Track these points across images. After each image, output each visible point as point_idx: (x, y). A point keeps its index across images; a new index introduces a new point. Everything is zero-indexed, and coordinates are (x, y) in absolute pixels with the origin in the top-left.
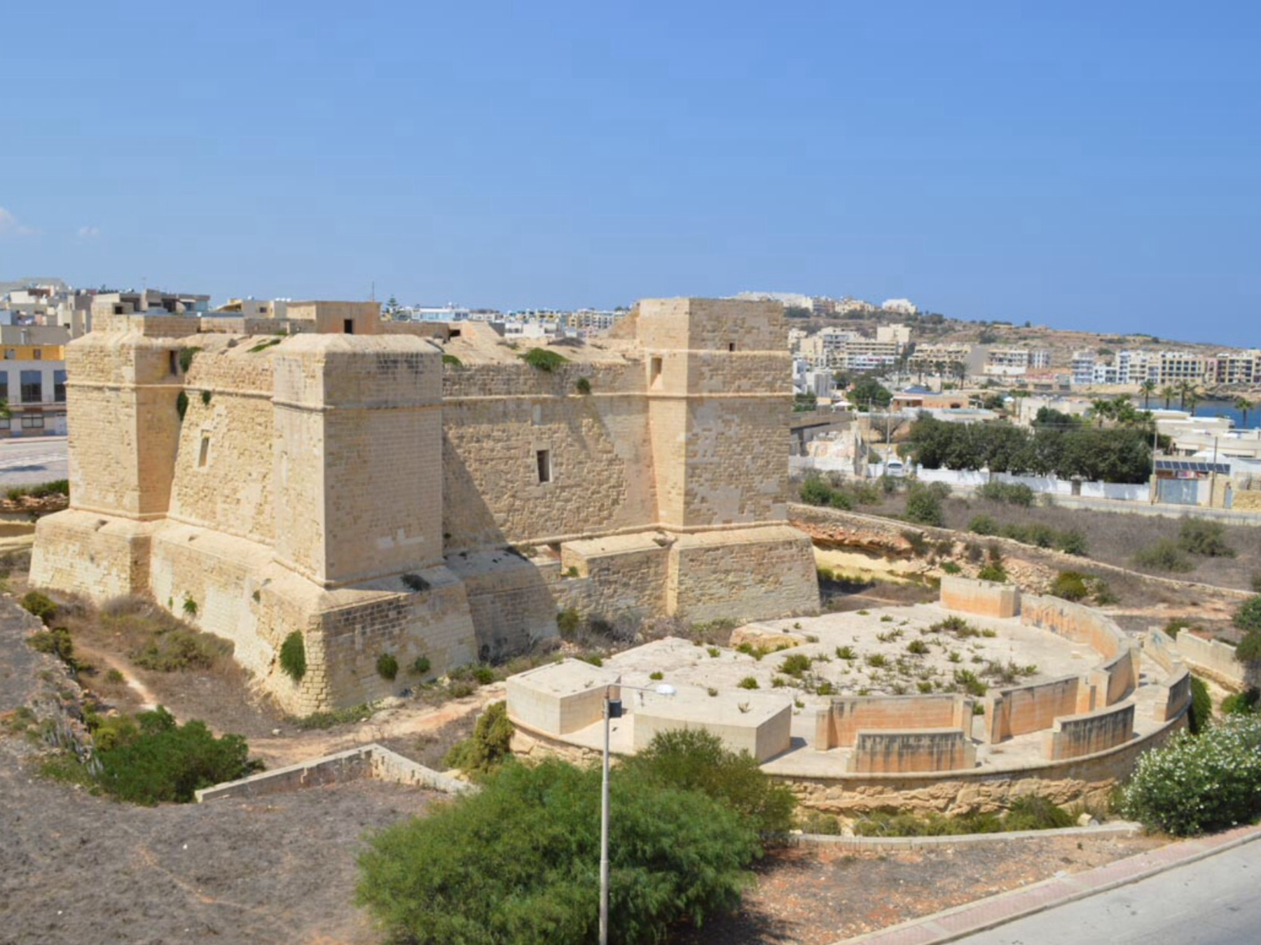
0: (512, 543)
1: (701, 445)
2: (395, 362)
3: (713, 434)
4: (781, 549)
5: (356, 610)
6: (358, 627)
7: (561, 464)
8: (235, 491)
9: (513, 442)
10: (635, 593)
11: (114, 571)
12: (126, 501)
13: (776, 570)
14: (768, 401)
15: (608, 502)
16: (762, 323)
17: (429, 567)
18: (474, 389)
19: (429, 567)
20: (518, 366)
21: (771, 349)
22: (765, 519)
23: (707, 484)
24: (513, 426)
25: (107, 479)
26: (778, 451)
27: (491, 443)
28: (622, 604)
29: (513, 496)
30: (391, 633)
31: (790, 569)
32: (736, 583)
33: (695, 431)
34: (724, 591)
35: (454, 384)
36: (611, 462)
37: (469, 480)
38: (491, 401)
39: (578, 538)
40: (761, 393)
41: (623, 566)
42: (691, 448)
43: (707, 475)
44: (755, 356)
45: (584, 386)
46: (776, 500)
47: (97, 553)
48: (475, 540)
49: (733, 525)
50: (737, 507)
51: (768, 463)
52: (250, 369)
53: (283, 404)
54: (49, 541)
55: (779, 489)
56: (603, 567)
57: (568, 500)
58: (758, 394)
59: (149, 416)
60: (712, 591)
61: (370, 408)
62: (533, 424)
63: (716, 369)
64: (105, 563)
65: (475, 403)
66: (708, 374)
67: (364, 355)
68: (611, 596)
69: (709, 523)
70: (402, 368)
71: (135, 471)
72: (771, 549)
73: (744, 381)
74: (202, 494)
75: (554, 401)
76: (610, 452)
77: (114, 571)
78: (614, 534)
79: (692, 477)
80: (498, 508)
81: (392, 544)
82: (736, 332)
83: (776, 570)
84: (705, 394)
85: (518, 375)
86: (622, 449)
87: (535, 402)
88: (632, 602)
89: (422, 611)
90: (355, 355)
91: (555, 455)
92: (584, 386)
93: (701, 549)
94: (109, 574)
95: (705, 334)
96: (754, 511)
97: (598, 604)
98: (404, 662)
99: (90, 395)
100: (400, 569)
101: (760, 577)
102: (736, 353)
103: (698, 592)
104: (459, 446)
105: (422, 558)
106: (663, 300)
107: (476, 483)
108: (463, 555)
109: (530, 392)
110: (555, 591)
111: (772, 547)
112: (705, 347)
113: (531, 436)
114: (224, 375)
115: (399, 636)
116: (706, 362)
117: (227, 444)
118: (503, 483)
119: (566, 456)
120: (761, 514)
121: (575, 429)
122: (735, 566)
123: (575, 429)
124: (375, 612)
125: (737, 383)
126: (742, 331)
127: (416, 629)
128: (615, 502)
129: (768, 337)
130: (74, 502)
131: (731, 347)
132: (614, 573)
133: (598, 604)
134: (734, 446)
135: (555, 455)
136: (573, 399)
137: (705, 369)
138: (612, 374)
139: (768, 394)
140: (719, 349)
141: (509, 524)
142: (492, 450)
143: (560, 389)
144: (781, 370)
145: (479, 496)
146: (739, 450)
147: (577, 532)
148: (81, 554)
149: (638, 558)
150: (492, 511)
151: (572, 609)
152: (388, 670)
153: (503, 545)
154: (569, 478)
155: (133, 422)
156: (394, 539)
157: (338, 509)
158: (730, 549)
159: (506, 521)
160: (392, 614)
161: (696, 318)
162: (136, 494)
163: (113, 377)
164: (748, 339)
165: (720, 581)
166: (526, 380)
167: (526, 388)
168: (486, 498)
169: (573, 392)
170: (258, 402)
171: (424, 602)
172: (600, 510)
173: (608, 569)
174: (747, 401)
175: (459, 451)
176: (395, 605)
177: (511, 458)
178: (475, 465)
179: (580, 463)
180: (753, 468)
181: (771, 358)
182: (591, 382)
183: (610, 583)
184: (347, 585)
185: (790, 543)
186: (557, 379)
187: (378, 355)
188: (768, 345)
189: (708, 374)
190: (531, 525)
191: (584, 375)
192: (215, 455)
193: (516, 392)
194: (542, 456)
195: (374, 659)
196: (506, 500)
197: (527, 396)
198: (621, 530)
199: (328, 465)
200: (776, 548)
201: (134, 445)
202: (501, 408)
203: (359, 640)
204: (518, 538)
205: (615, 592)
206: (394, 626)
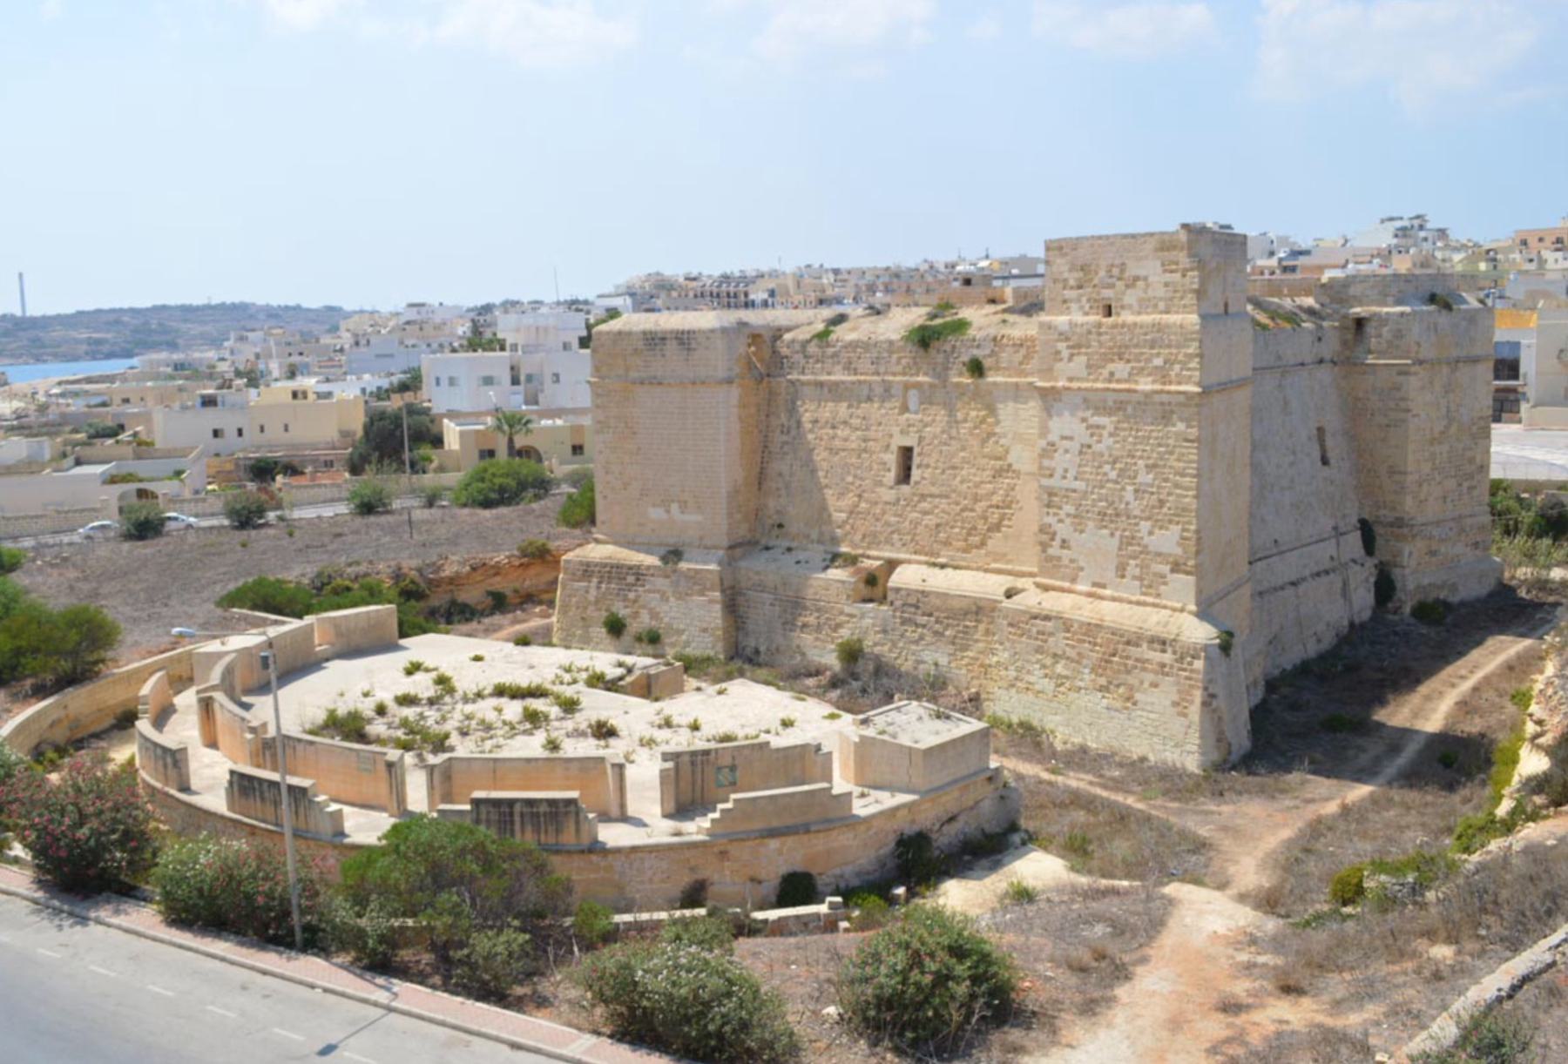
0: (844, 549)
1: (1060, 461)
2: (663, 339)
3: (1075, 446)
4: (1145, 645)
5: (596, 565)
6: (595, 580)
7: (928, 466)
9: (871, 434)
10: (951, 649)
13: (1131, 680)
14: (1157, 398)
15: (982, 527)
16: (1151, 269)
17: (706, 547)
18: (839, 367)
19: (706, 547)
20: (891, 343)
21: (1167, 312)
22: (1158, 595)
23: (1068, 521)
24: (874, 410)
26: (1177, 486)
27: (847, 432)
28: (928, 656)
29: (860, 496)
31: (1155, 685)
32: (1067, 677)
33: (1053, 437)
34: (1048, 685)
35: (817, 361)
36: (998, 473)
37: (814, 471)
38: (853, 383)
39: (927, 563)
40: (1145, 385)
41: (938, 609)
42: (1046, 463)
44: (1135, 324)
45: (977, 368)
46: (1176, 568)
48: (808, 536)
49: (1107, 592)
50: (1113, 567)
51: (1162, 503)
55: (1179, 551)
56: (918, 604)
57: (926, 513)
58: (1140, 387)
60: (1032, 679)
61: (634, 383)
62: (905, 409)
63: (1079, 346)
65: (837, 384)
66: (1065, 354)
67: (629, 334)
68: (916, 642)
69: (1074, 580)
70: (672, 346)
72: (1128, 643)
73: (1121, 369)
75: (931, 386)
76: (999, 459)
78: (978, 569)
79: (1048, 506)
80: (838, 507)
81: (664, 516)
82: (1112, 286)
83: (1131, 680)
84: (1060, 384)
85: (891, 352)
86: (1022, 458)
87: (907, 387)
88: (943, 661)
89: (661, 583)
90: (620, 333)
91: (920, 454)
92: (977, 368)
93: (1024, 612)
95: (1069, 294)
96: (1141, 579)
97: (894, 645)
98: (634, 627)
100: (671, 541)
101: (1103, 681)
102: (1111, 320)
103: (1013, 674)
104: (811, 431)
105: (701, 538)
107: (821, 474)
108: (789, 549)
109: (904, 374)
110: (842, 613)
111: (1133, 641)
112: (1068, 311)
113: (894, 427)
115: (635, 601)
116: (1064, 337)
118: (850, 479)
119: (935, 456)
120: (1151, 584)
121: (953, 422)
122: (1071, 653)
123: (953, 422)
124: (614, 572)
125: (1111, 367)
126: (1120, 285)
127: (653, 600)
128: (997, 527)
129: (1161, 292)
131: (1108, 311)
132: (924, 614)
133: (894, 645)
134: (1107, 468)
135: (920, 454)
136: (958, 385)
137: (1062, 346)
138: (1023, 351)
139: (1158, 387)
140: (1087, 314)
141: (848, 527)
142: (846, 440)
143: (942, 374)
144: (1179, 346)
145: (821, 489)
146: (1113, 475)
147: (932, 554)
149: (964, 604)
150: (832, 509)
151: (860, 641)
152: (615, 628)
153: (835, 550)
154: (933, 484)
156: (668, 512)
158: (1067, 625)
159: (845, 522)
160: (631, 579)
161: (1054, 269)
164: (1130, 298)
165: (1044, 667)
166: (898, 362)
167: (899, 368)
168: (828, 492)
169: (961, 374)
171: (667, 577)
172: (969, 534)
173: (917, 607)
174: (1123, 396)
175: (810, 437)
176: (638, 573)
177: (865, 450)
178: (825, 454)
179: (954, 468)
180: (1136, 507)
181: (1159, 328)
182: (987, 363)
183: (917, 625)
184: (615, 543)
185: (1164, 643)
186: (940, 358)
187: (644, 333)
188: (1162, 305)
189: (1065, 354)
190: (874, 535)
191: (976, 352)
193: (886, 373)
194: (907, 453)
195: (605, 614)
196: (850, 499)
197: (898, 378)
198: (994, 565)
200: (1137, 645)
202: (865, 392)
203: (593, 592)
204: (855, 546)
205: (921, 638)
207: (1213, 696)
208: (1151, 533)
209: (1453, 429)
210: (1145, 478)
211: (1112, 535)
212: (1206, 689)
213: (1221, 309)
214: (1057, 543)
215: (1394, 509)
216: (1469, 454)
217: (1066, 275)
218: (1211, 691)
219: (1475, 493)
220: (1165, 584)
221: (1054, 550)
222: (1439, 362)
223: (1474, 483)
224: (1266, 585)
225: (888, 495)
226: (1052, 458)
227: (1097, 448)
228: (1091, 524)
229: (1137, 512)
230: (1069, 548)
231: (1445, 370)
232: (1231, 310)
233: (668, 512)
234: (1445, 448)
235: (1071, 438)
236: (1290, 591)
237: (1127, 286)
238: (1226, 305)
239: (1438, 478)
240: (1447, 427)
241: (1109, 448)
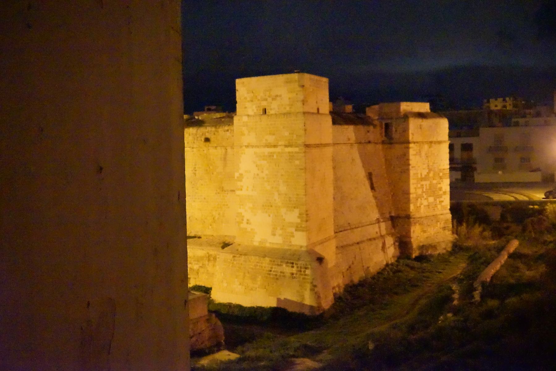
55: (299, 221)
66: (246, 132)
82: (266, 100)
189: (246, 132)
207: (315, 286)
209: (431, 175)
211: (269, 216)
212: (312, 283)
213: (316, 111)
214: (245, 221)
215: (405, 210)
216: (439, 186)
218: (314, 284)
219: (443, 204)
220: (293, 236)
221: (244, 225)
222: (423, 142)
223: (442, 199)
224: (345, 243)
226: (241, 181)
229: (280, 204)
230: (250, 224)
231: (426, 147)
232: (321, 111)
234: (428, 183)
236: (357, 246)
237: (273, 99)
238: (318, 109)
239: (425, 197)
240: (429, 173)
241: (267, 175)
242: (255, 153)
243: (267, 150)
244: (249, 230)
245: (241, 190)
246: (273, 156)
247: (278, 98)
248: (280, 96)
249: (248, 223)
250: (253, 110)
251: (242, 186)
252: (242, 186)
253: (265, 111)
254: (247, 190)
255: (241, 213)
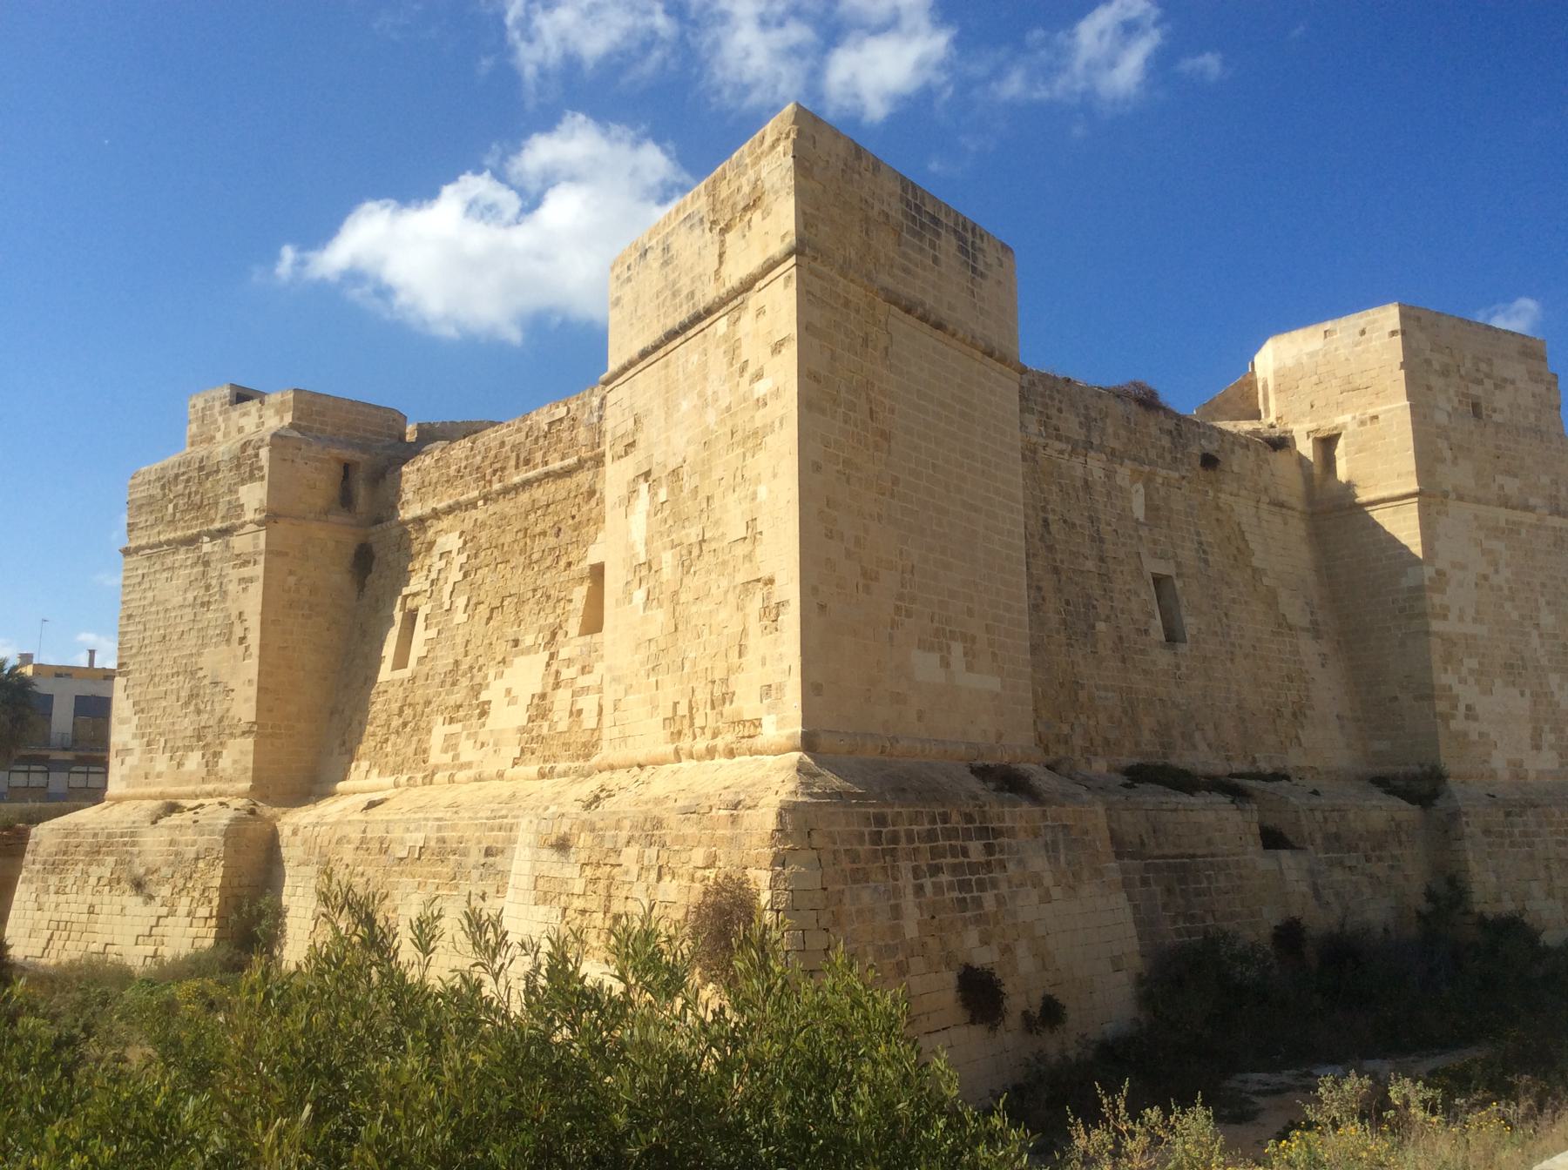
8: (476, 690)
11: (183, 904)
12: (225, 762)
25: (187, 724)
30: (978, 903)
33: (1440, 564)
43: (1473, 663)
47: (149, 872)
52: (521, 437)
53: (644, 354)
54: (55, 866)
59: (292, 580)
64: (165, 891)
70: (948, 243)
71: (252, 691)
74: (396, 722)
77: (183, 904)
82: (1480, 382)
94: (172, 913)
95: (1436, 381)
99: (169, 561)
106: (1328, 325)
114: (460, 475)
117: (461, 602)
130: (115, 787)
134: (1508, 606)
148: (114, 882)
155: (256, 590)
156: (945, 663)
157: (830, 535)
162: (249, 743)
163: (222, 508)
170: (538, 493)
189: (1448, 454)
192: (432, 633)
199: (806, 404)
201: (254, 639)
206: (981, 886)
208: (1561, 687)
210: (1547, 619)
211: (1522, 694)
217: (1428, 354)
225: (1163, 658)
226: (1443, 592)
227: (1496, 580)
228: (1498, 682)
230: (1476, 719)
233: (945, 663)
235: (1463, 567)
241: (1507, 581)
242: (1476, 517)
243: (1503, 514)
244: (1474, 737)
245: (1445, 617)
246: (1519, 533)
247: (1510, 388)
248: (1513, 382)
249: (1467, 717)
250: (1449, 400)
251: (1447, 608)
252: (1447, 608)
253: (1476, 409)
254: (1461, 619)
255: (1450, 688)
